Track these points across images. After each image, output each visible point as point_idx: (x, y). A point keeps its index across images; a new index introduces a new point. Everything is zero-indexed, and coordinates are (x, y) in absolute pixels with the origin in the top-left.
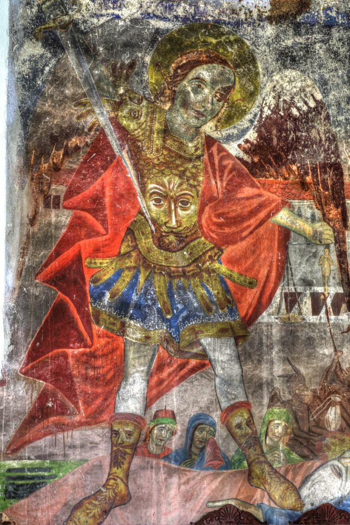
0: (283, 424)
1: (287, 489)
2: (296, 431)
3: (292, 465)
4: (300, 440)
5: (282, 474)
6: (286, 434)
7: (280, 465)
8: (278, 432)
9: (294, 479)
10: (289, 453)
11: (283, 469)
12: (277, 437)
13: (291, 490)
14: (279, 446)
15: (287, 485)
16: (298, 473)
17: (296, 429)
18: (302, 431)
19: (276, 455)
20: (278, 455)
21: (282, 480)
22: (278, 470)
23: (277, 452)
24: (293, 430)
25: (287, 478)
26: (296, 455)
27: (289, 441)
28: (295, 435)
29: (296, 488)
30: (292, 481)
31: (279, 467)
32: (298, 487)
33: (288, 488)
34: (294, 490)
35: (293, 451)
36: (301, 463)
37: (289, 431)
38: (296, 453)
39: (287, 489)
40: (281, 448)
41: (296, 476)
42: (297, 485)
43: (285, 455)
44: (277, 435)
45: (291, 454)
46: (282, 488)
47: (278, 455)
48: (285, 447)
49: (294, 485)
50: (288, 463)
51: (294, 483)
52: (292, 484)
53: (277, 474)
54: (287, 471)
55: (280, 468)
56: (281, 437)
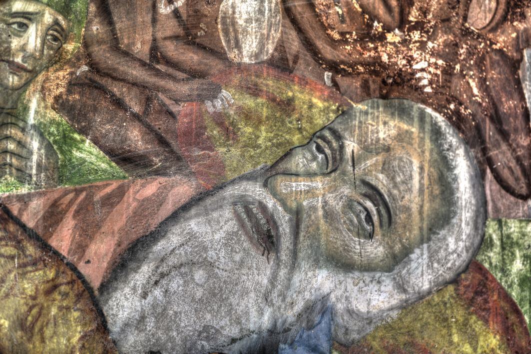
0: (48, 18)
1: (48, 292)
2: (101, 53)
3: (78, 192)
4: (117, 89)
5: (31, 224)
6: (57, 59)
7: (24, 190)
8: (23, 49)
9: (81, 248)
10: (66, 141)
11: (37, 205)
12: (17, 69)
13: (66, 295)
14: (26, 109)
15: (51, 274)
16: (98, 226)
17: (100, 42)
18: (126, 54)
19: (11, 146)
20: (20, 143)
21: (31, 250)
22: (15, 209)
23: (13, 131)
24: (86, 45)
25: (54, 243)
26: (95, 150)
27: (69, 91)
28: (94, 67)
29: (89, 289)
30: (70, 258)
31: (22, 199)
32: (96, 284)
33: (52, 288)
34: (79, 296)
35: (83, 131)
36: (114, 185)
37: (70, 47)
38: (96, 142)
39: (48, 292)
40: (31, 120)
41: (92, 238)
42: (94, 273)
43: (49, 147)
44: (18, 60)
45: (74, 143)
46: (28, 287)
47: (20, 143)
48: (52, 114)
49: (80, 276)
50: (61, 181)
51: (82, 268)
52: (74, 269)
53: (12, 227)
54: (53, 215)
55: (24, 200)
56: (34, 73)
